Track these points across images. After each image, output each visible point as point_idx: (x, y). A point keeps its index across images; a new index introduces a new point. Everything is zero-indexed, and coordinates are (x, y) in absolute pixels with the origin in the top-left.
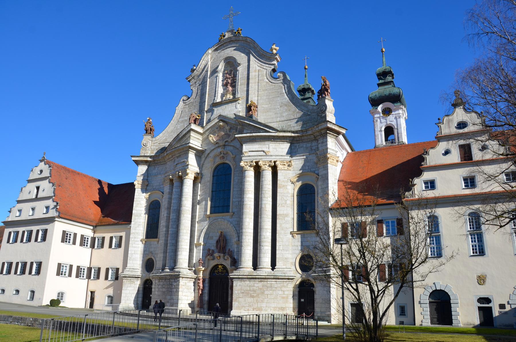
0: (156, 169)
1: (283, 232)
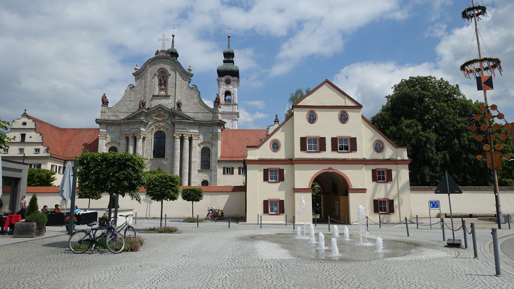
0: (113, 128)
1: (194, 170)
